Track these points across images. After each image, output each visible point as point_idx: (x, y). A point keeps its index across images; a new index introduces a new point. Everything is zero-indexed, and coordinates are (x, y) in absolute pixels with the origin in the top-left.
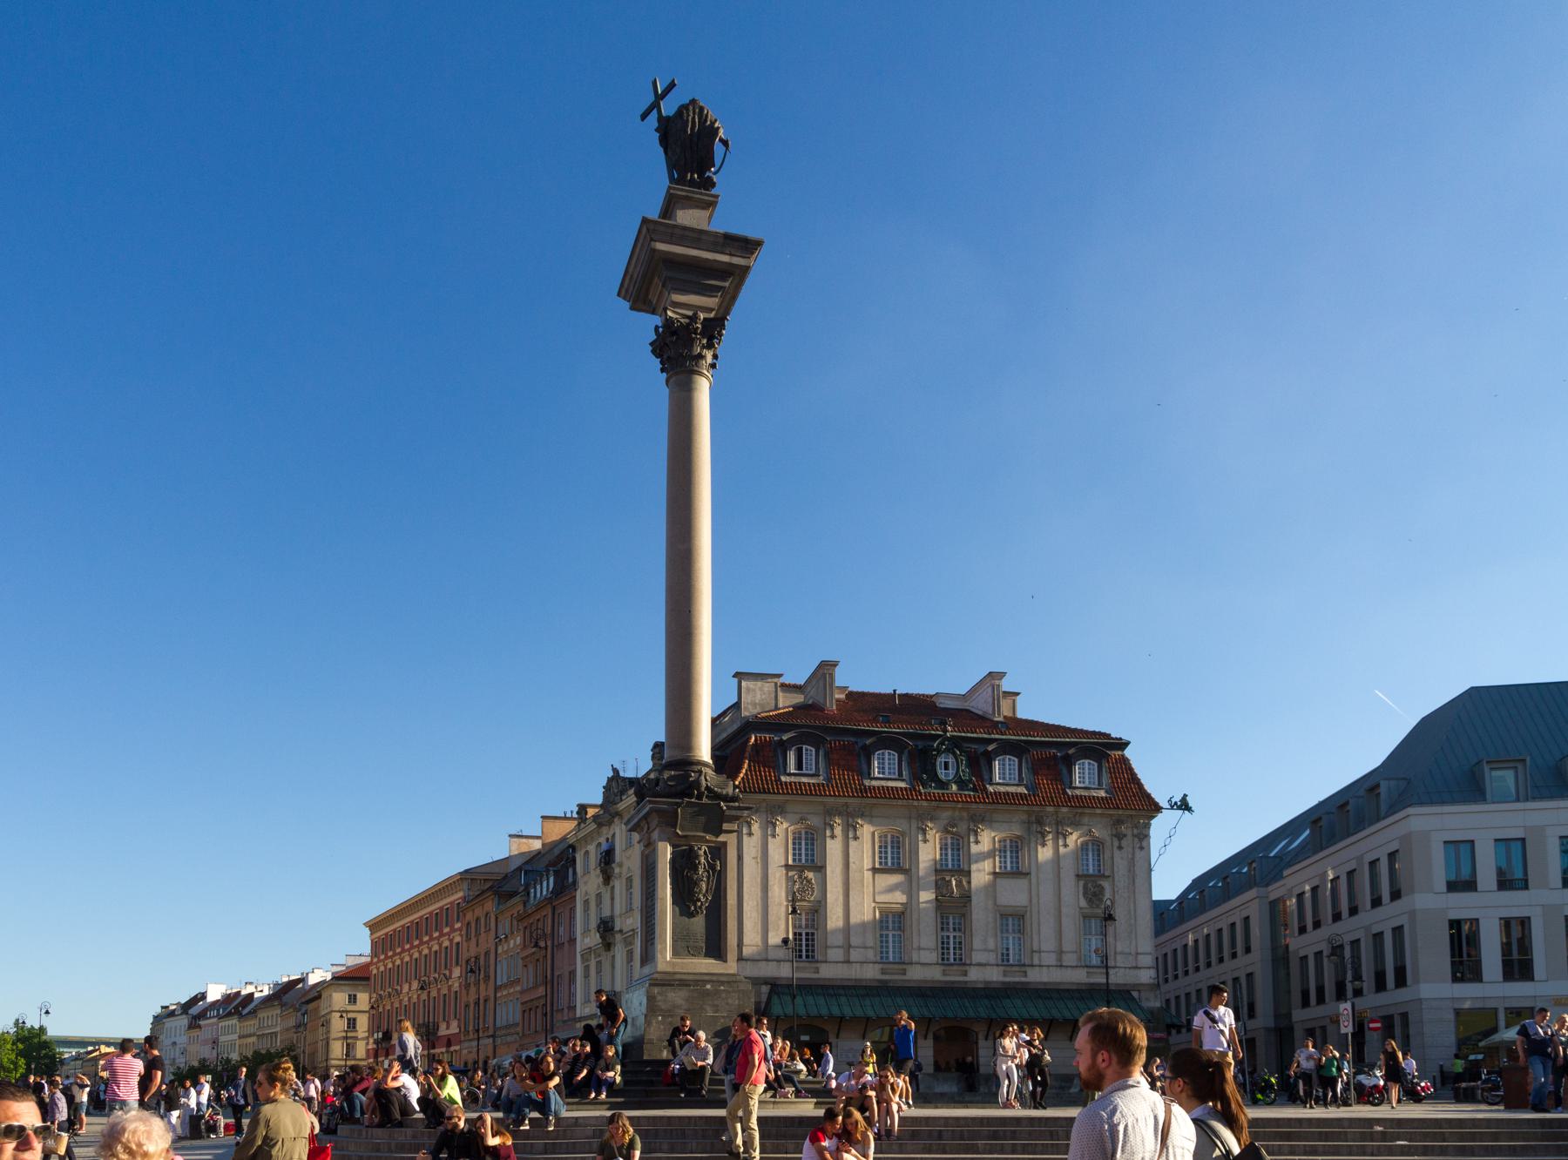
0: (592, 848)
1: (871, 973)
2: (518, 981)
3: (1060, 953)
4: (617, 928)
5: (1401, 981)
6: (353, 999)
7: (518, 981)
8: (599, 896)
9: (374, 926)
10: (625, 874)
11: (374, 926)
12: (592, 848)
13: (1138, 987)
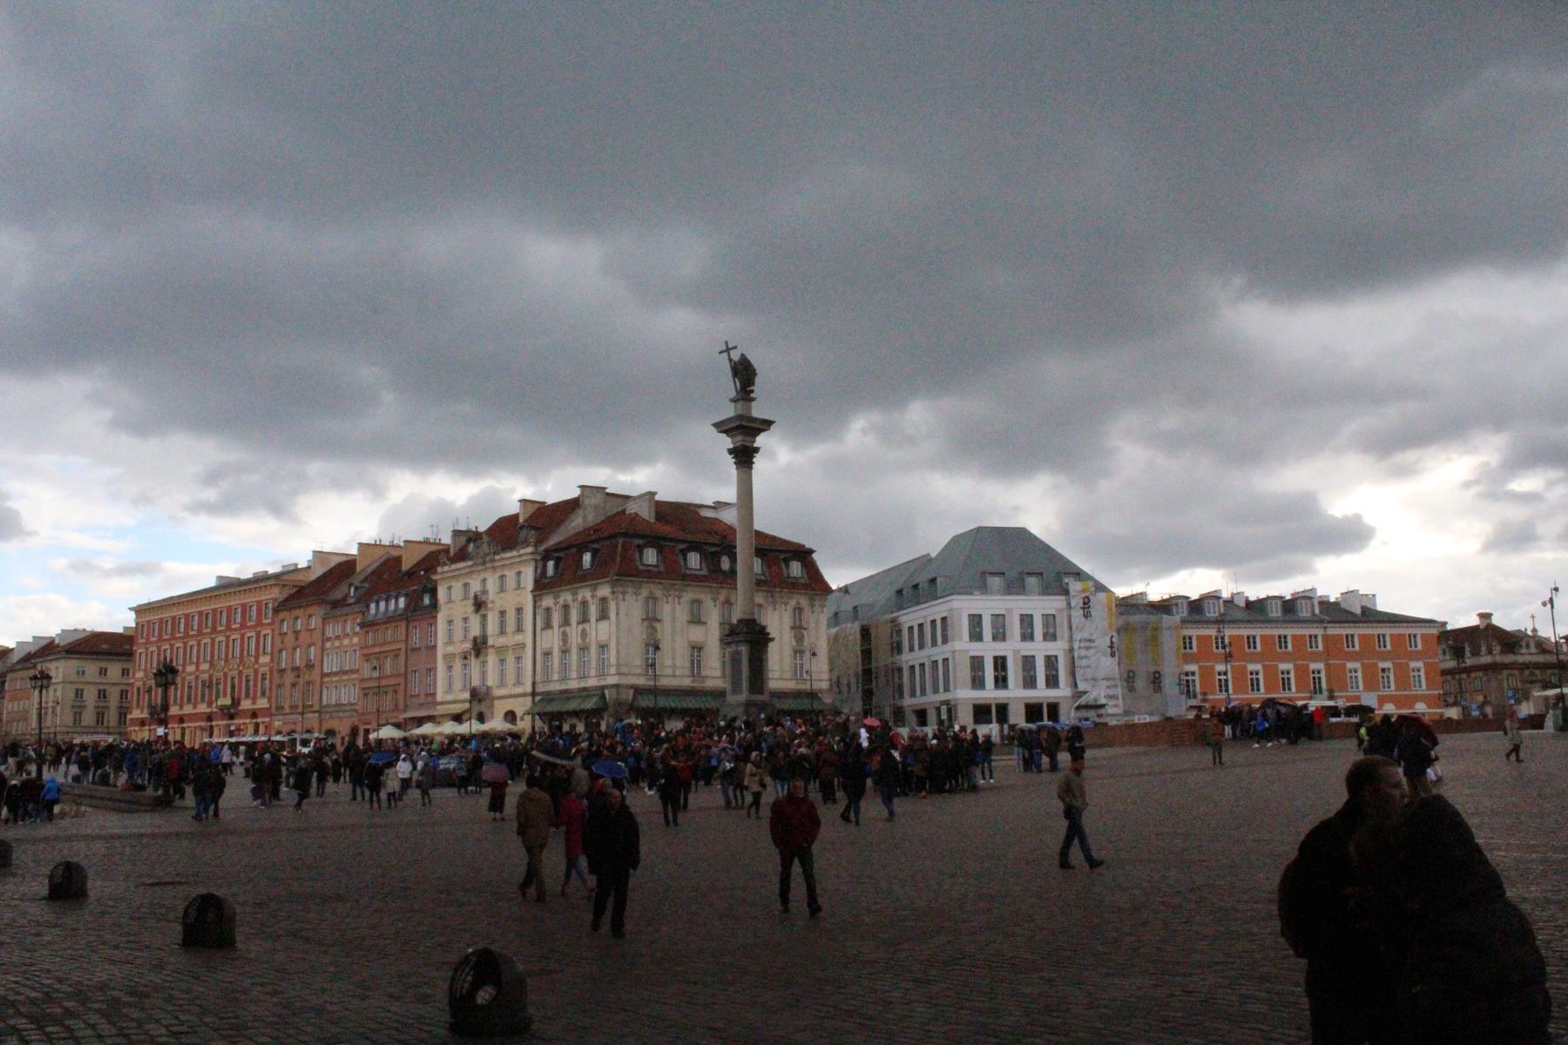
0: (457, 586)
1: (686, 682)
2: (356, 671)
3: (782, 671)
4: (490, 642)
5: (947, 689)
6: (103, 672)
7: (356, 671)
8: (466, 620)
9: (140, 610)
10: (498, 606)
11: (140, 610)
12: (457, 586)
13: (821, 691)
